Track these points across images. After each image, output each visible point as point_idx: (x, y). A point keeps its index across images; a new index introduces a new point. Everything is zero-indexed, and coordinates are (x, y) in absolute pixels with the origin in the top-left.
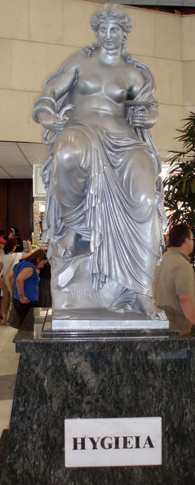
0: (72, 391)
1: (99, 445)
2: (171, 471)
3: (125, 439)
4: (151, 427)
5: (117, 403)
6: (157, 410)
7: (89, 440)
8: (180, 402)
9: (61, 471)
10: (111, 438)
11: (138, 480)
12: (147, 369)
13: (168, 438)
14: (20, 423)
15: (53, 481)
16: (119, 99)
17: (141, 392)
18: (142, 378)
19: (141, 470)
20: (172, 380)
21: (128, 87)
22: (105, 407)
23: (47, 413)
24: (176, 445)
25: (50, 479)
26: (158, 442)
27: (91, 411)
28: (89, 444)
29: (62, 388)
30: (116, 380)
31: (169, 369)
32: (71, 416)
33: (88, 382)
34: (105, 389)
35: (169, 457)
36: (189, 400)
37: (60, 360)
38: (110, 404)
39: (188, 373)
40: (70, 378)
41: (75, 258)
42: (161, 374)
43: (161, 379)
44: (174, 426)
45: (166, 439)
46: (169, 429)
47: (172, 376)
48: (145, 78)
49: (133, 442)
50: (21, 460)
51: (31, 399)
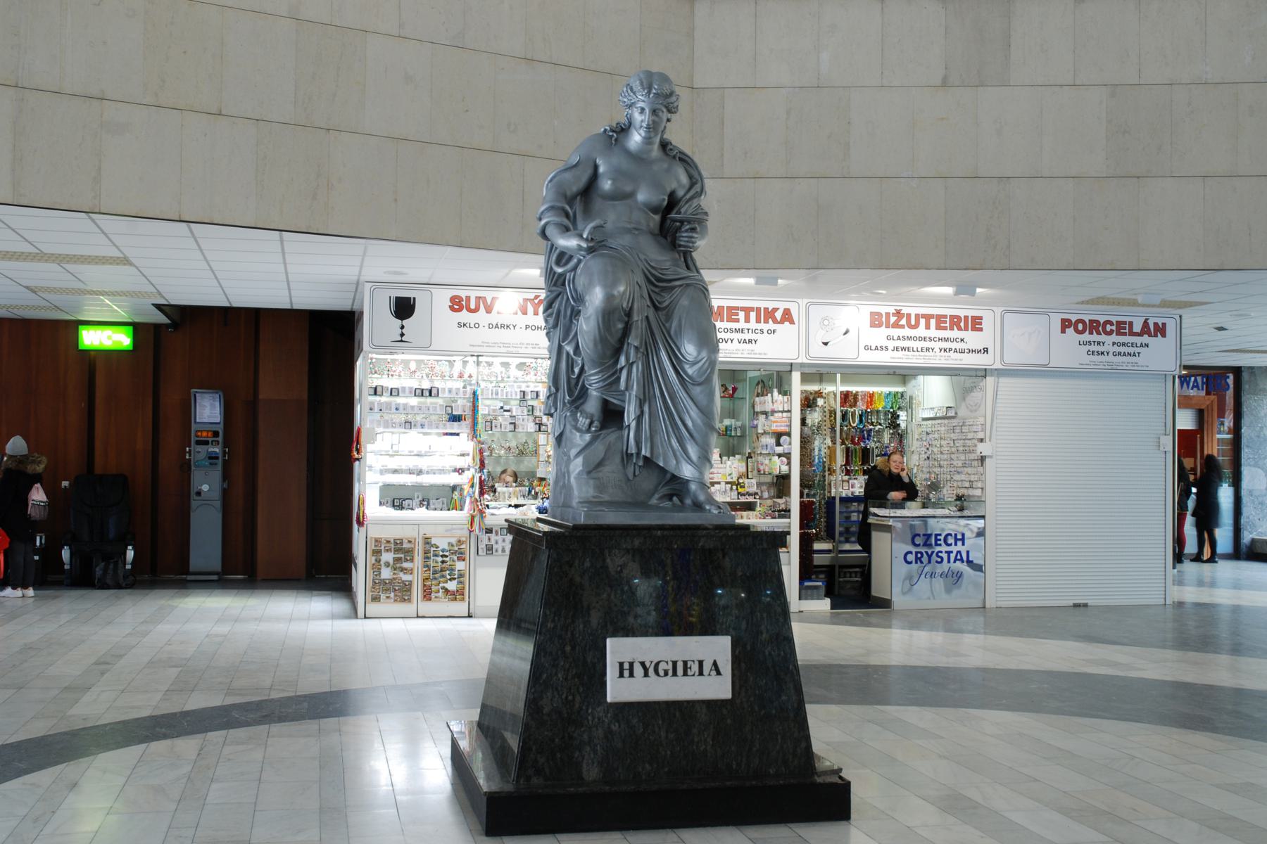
1: (651, 671)
3: (685, 663)
4: (718, 648)
16: (655, 210)
21: (669, 190)
28: (638, 670)
32: (614, 635)
41: (604, 432)
48: (690, 177)
49: (695, 668)
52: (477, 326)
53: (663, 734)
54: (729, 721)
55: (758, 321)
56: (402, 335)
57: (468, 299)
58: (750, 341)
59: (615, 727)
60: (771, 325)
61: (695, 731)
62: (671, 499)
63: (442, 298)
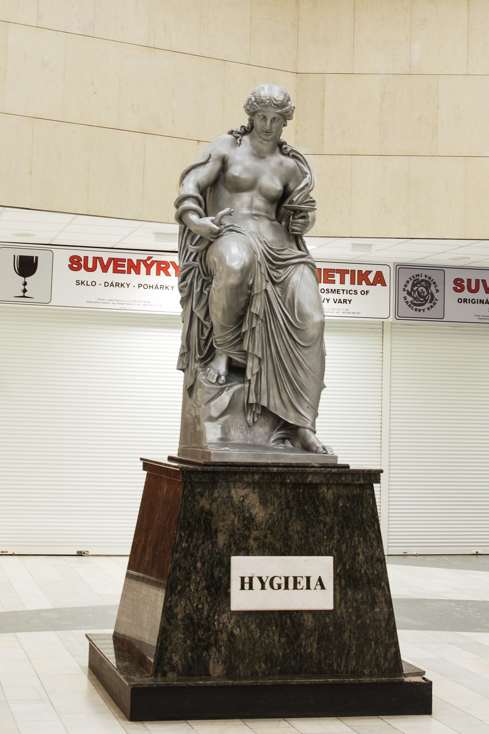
0: (238, 526)
1: (267, 585)
2: (343, 618)
3: (295, 578)
4: (322, 566)
6: (328, 549)
7: (257, 579)
9: (227, 616)
10: (280, 578)
11: (307, 627)
12: (318, 503)
13: (340, 581)
14: (183, 560)
15: (216, 627)
17: (312, 529)
18: (313, 513)
19: (310, 616)
22: (274, 544)
23: (212, 550)
25: (214, 624)
26: (329, 583)
27: (259, 547)
28: (257, 584)
30: (285, 515)
31: (341, 504)
32: (237, 554)
33: (256, 516)
34: (274, 523)
35: (341, 602)
36: (361, 539)
37: (226, 491)
39: (360, 509)
40: (236, 511)
41: (229, 384)
42: (332, 510)
43: (332, 515)
44: (345, 567)
45: (337, 581)
46: (340, 571)
47: (344, 512)
49: (304, 583)
52: (94, 283)
53: (276, 638)
54: (331, 629)
55: (352, 282)
56: (25, 291)
57: (86, 258)
58: (345, 301)
59: (237, 632)
60: (364, 287)
61: (303, 636)
62: (283, 442)
63: (62, 258)
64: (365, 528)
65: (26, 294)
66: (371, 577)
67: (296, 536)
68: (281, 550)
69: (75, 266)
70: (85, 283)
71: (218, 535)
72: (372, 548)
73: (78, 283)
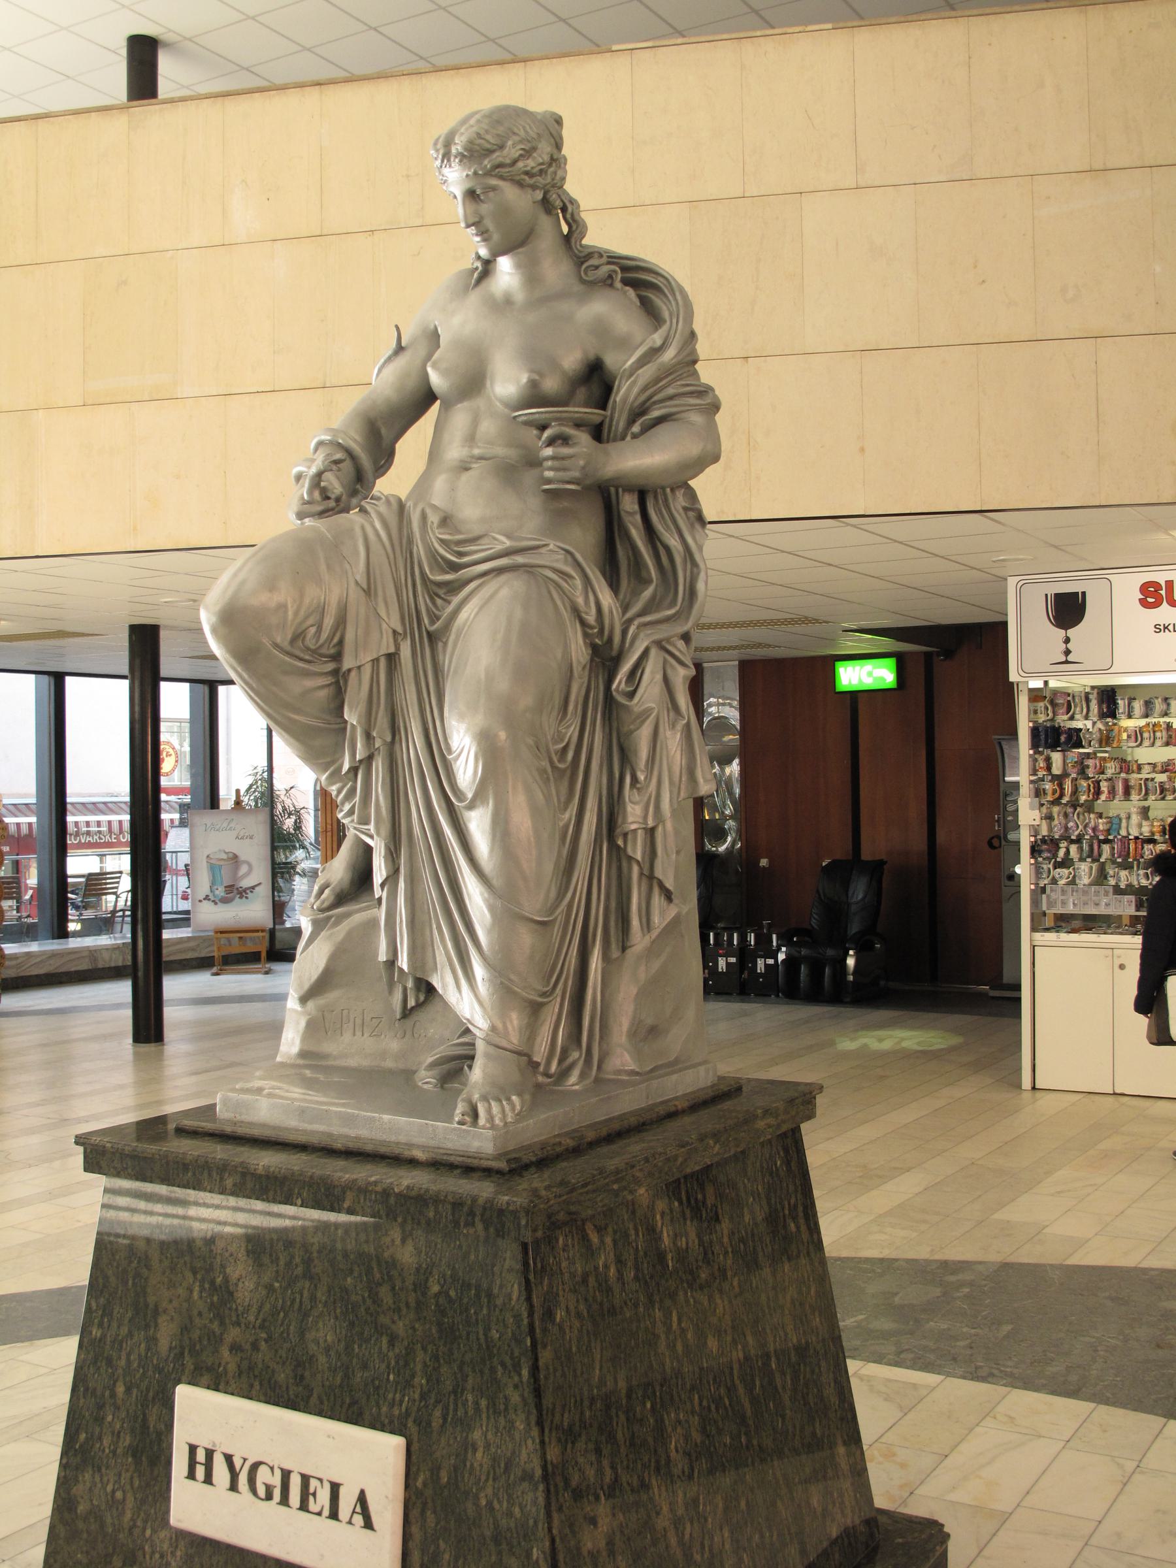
3: (305, 1479)
5: (299, 1364)
8: (460, 1405)
12: (378, 1276)
17: (360, 1346)
20: (440, 1324)
23: (146, 1357)
24: (441, 1542)
25: (143, 1549)
29: (180, 1291)
31: (435, 1288)
33: (236, 1285)
36: (483, 1403)
38: (284, 1363)
39: (485, 1311)
43: (412, 1316)
44: (438, 1478)
46: (425, 1484)
47: (442, 1312)
49: (324, 1496)
50: (87, 1476)
51: (117, 1309)
56: (1067, 652)
63: (1127, 587)
64: (493, 1370)
65: (1070, 658)
66: (503, 1522)
67: (322, 1359)
68: (287, 1388)
69: (1151, 600)
70: (1171, 628)
71: (160, 1320)
72: (512, 1438)
73: (1158, 629)
